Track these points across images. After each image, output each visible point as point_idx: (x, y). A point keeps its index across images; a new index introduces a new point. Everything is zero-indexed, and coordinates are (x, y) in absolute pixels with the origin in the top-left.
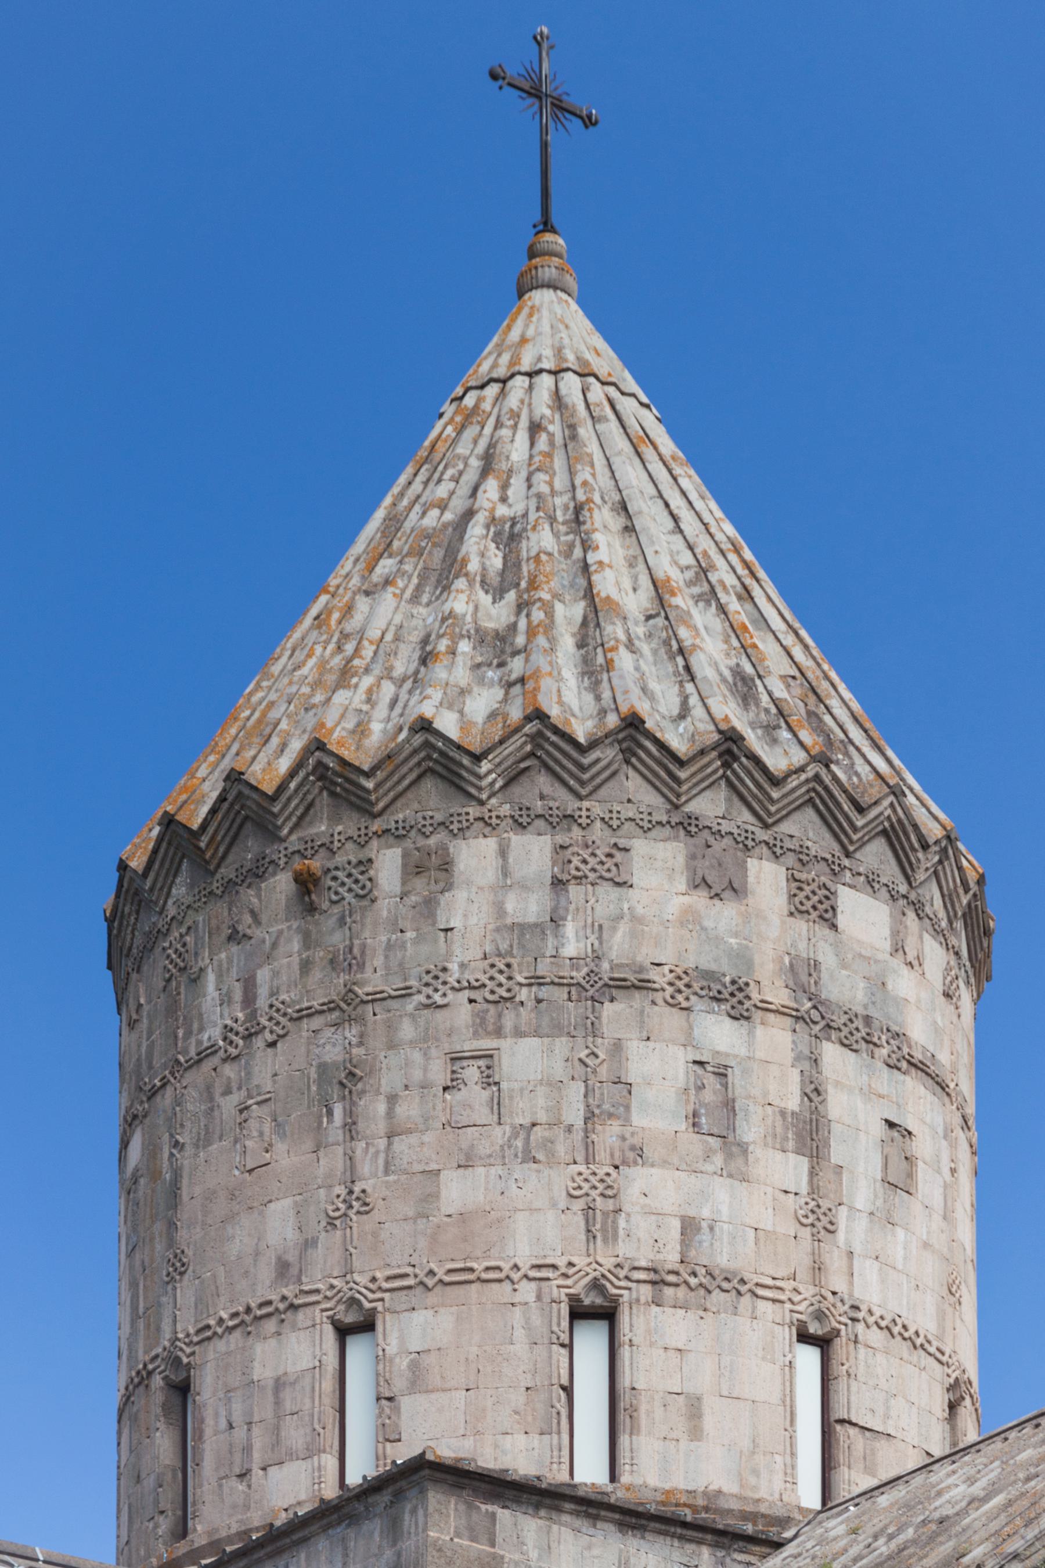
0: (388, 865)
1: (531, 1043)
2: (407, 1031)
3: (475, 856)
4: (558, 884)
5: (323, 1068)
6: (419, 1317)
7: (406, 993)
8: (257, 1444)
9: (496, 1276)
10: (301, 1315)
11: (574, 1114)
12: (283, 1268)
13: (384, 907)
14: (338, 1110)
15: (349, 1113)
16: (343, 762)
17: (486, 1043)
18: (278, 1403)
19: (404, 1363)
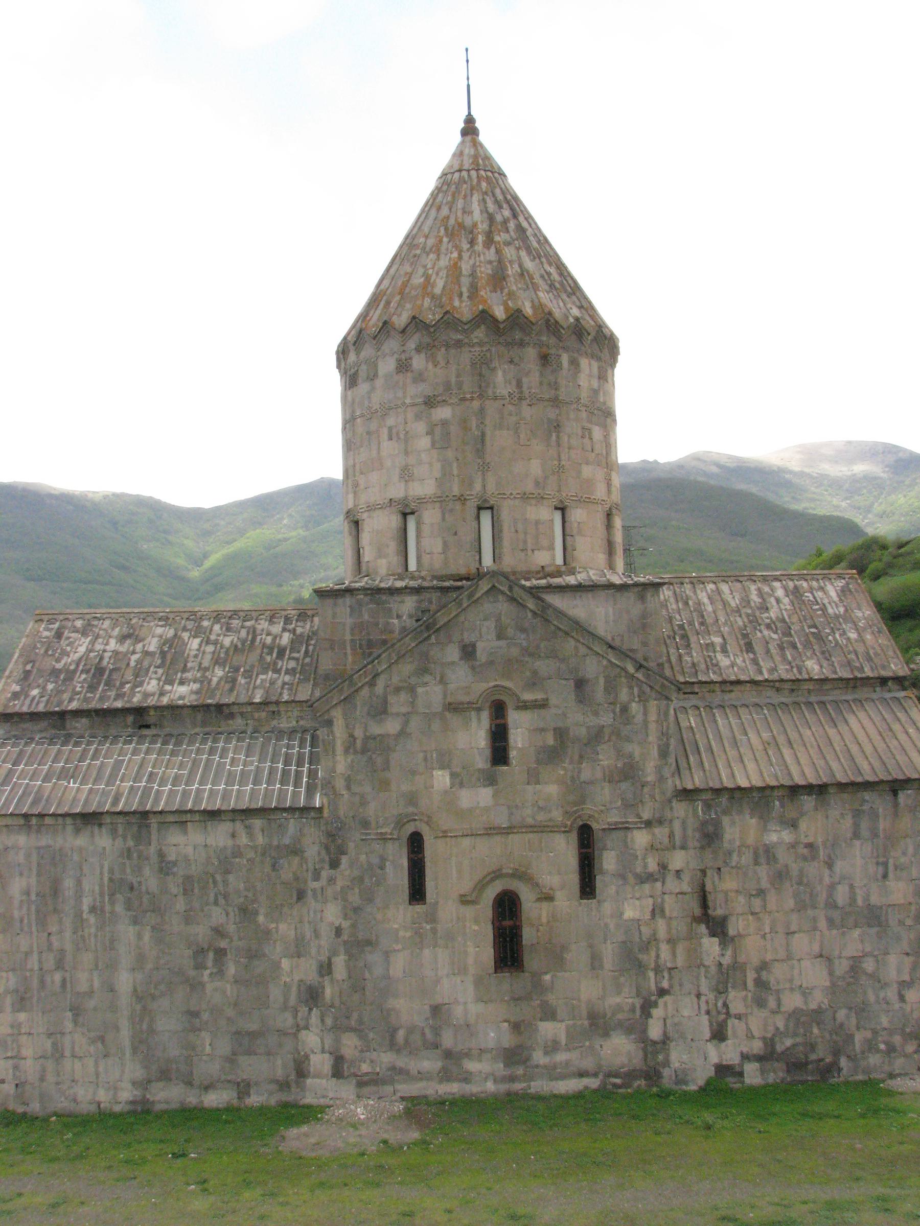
0: (565, 359)
1: (597, 427)
2: (572, 416)
3: (584, 362)
4: (599, 378)
5: (548, 419)
6: (579, 511)
7: (571, 403)
8: (529, 541)
9: (594, 502)
10: (545, 501)
11: (604, 453)
12: (537, 484)
13: (564, 372)
14: (554, 437)
15: (558, 437)
16: (556, 322)
17: (589, 426)
18: (537, 529)
19: (576, 525)
